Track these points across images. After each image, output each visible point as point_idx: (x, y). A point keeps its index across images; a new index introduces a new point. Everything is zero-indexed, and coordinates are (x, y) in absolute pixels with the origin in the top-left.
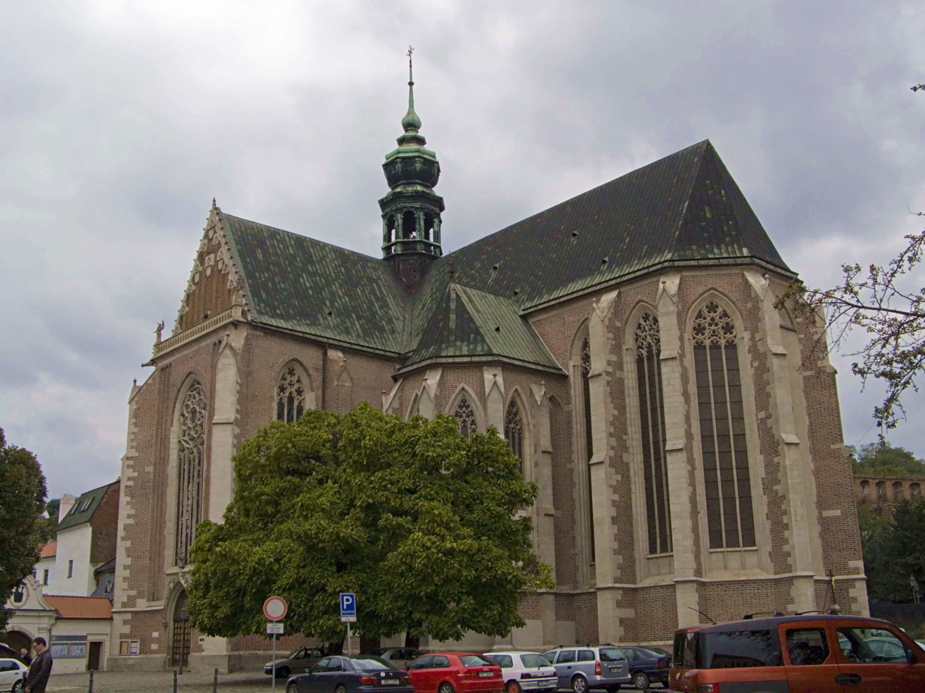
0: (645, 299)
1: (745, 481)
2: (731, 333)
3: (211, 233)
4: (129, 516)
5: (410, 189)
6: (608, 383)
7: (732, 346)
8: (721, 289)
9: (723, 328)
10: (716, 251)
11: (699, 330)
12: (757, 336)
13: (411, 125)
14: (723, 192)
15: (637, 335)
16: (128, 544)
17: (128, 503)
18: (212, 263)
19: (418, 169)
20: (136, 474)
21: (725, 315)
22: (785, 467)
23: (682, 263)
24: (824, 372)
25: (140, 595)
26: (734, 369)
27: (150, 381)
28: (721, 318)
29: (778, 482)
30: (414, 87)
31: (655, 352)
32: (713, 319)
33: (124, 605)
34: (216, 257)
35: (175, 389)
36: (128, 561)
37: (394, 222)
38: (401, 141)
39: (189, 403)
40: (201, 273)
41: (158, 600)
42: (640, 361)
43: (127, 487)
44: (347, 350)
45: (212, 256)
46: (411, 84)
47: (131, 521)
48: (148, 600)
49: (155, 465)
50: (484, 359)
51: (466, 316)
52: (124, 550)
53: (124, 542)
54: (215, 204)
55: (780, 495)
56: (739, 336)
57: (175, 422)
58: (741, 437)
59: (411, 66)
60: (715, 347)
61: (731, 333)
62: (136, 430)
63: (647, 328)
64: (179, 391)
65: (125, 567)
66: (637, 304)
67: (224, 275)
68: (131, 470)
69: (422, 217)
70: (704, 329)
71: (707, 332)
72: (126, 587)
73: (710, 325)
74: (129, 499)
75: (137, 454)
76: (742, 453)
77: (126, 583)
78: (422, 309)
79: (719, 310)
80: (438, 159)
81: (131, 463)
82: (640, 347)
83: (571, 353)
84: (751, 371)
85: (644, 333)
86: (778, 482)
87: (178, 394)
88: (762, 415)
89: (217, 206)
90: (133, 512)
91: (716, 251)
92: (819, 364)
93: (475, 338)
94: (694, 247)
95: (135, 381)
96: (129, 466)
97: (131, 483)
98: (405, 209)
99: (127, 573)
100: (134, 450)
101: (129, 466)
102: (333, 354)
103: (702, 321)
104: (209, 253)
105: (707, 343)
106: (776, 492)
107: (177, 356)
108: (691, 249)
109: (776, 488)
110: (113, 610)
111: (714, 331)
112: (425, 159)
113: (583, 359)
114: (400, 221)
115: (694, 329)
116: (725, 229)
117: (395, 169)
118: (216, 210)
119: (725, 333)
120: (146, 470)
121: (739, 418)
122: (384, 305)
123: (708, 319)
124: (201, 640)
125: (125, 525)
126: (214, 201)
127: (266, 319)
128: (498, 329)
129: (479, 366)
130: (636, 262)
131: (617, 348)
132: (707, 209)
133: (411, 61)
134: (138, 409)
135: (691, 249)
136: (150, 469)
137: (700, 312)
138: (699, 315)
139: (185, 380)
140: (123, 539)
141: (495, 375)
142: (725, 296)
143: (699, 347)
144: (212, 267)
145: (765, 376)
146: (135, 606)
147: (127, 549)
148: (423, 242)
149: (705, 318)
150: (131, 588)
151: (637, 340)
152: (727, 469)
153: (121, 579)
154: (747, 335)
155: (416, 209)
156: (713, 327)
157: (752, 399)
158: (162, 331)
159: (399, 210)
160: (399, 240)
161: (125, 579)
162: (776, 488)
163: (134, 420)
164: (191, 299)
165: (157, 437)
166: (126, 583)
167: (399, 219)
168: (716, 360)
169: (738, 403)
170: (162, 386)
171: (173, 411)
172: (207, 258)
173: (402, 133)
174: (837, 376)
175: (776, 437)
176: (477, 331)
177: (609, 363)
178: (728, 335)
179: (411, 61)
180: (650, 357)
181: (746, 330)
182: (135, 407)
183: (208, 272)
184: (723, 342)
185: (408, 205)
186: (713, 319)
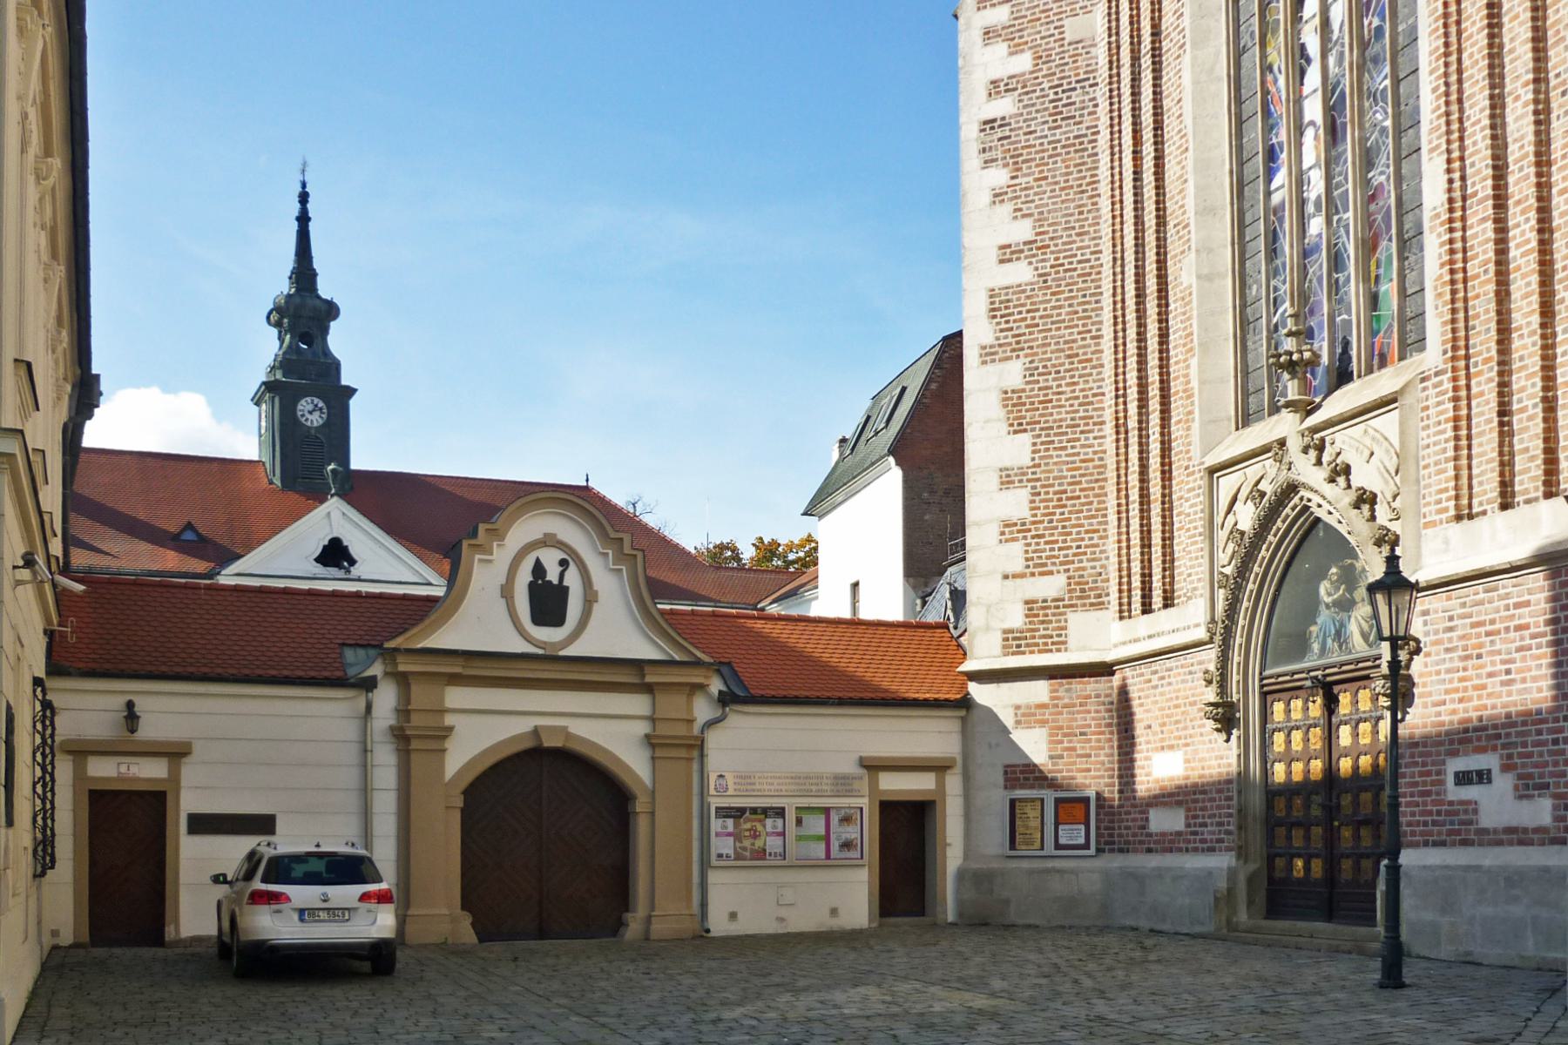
4: (1008, 254)
16: (1013, 373)
17: (998, 196)
25: (1085, 595)
33: (1014, 641)
36: (1019, 450)
41: (1168, 602)
47: (1021, 273)
48: (1124, 613)
52: (995, 398)
53: (998, 367)
65: (1008, 480)
68: (1001, 48)
72: (1018, 565)
74: (999, 176)
77: (1017, 548)
90: (1023, 231)
99: (1017, 503)
110: (969, 666)
120: (1069, 37)
124: (1463, 778)
125: (992, 294)
140: (989, 355)
146: (1061, 645)
147: (1012, 400)
150: (1037, 567)
153: (994, 530)
161: (1011, 530)
166: (1017, 548)
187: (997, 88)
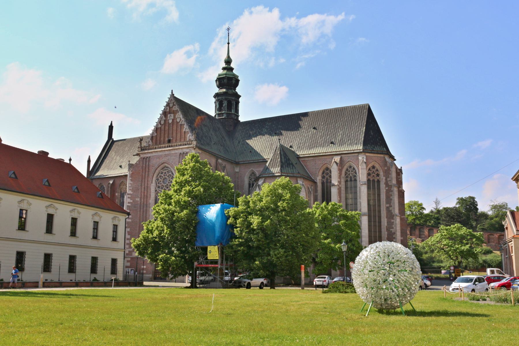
0: (352, 161)
1: (380, 226)
2: (379, 177)
3: (171, 105)
5: (230, 91)
6: (338, 189)
7: (379, 181)
8: (377, 162)
9: (376, 175)
10: (376, 148)
11: (369, 174)
12: (388, 179)
13: (228, 61)
14: (376, 125)
15: (346, 172)
18: (172, 118)
19: (234, 83)
20: (132, 201)
21: (377, 170)
22: (396, 224)
23: (367, 151)
24: (401, 192)
26: (379, 189)
27: (138, 163)
28: (376, 171)
29: (393, 228)
30: (230, 44)
31: (353, 179)
32: (373, 171)
34: (174, 116)
35: (154, 168)
37: (223, 104)
38: (224, 69)
39: (162, 175)
40: (165, 121)
42: (346, 181)
43: (128, 206)
44: (224, 159)
45: (172, 115)
46: (228, 43)
49: (141, 198)
50: (298, 175)
51: (287, 158)
54: (172, 92)
55: (393, 232)
56: (381, 178)
57: (154, 182)
58: (380, 211)
59: (229, 35)
60: (374, 181)
61: (379, 177)
62: (132, 182)
63: (351, 171)
64: (156, 169)
66: (348, 162)
67: (181, 125)
68: (129, 199)
69: (235, 104)
70: (371, 174)
71: (371, 175)
73: (372, 173)
75: (132, 193)
76: (380, 217)
78: (239, 142)
79: (376, 169)
80: (239, 78)
81: (130, 196)
82: (346, 177)
83: (318, 175)
84: (385, 191)
85: (349, 173)
86: (393, 228)
87: (156, 170)
88: (388, 205)
89: (173, 93)
91: (376, 148)
92: (400, 189)
93: (292, 167)
94: (369, 145)
95: (129, 161)
96: (129, 197)
97: (129, 205)
98: (228, 99)
100: (131, 191)
101: (129, 197)
102: (220, 161)
103: (369, 172)
104: (170, 113)
105: (372, 179)
106: (391, 231)
107: (154, 154)
108: (368, 146)
109: (391, 230)
111: (373, 175)
112: (236, 79)
113: (322, 177)
114: (226, 104)
115: (368, 174)
116: (378, 140)
117: (224, 81)
118: (172, 95)
119: (377, 176)
120: (136, 200)
121: (379, 206)
122: (225, 141)
123: (372, 171)
126: (172, 91)
127: (201, 146)
128: (296, 163)
129: (297, 177)
130: (346, 146)
131: (340, 177)
132: (371, 131)
133: (228, 33)
134: (132, 174)
135: (368, 146)
136: (138, 199)
137: (370, 168)
138: (369, 169)
139: (160, 165)
141: (303, 182)
142: (379, 164)
143: (369, 180)
144: (173, 120)
145: (391, 193)
146: (132, 255)
148: (235, 114)
149: (371, 171)
151: (346, 175)
152: (375, 222)
154: (384, 178)
155: (233, 100)
156: (373, 174)
157: (385, 200)
158: (142, 142)
159: (226, 99)
160: (226, 112)
162: (391, 230)
163: (131, 178)
164: (159, 130)
165: (141, 186)
167: (225, 104)
168: (374, 185)
169: (379, 200)
170: (144, 165)
171: (153, 177)
172: (169, 115)
173: (224, 65)
174: (405, 192)
175: (393, 214)
176: (292, 164)
177: (338, 182)
178: (378, 177)
179: (228, 33)
180: (351, 180)
181: (384, 176)
182: (131, 173)
183: (170, 121)
184: (376, 180)
185: (230, 98)
186: (373, 171)
187: (129, 203)
